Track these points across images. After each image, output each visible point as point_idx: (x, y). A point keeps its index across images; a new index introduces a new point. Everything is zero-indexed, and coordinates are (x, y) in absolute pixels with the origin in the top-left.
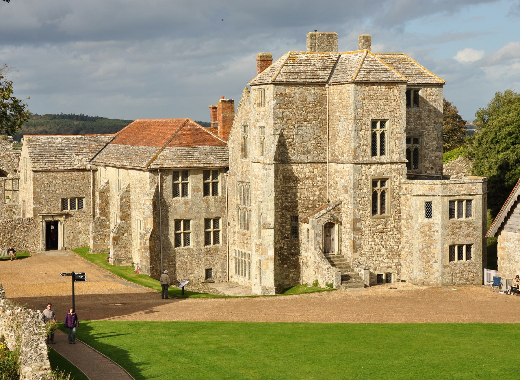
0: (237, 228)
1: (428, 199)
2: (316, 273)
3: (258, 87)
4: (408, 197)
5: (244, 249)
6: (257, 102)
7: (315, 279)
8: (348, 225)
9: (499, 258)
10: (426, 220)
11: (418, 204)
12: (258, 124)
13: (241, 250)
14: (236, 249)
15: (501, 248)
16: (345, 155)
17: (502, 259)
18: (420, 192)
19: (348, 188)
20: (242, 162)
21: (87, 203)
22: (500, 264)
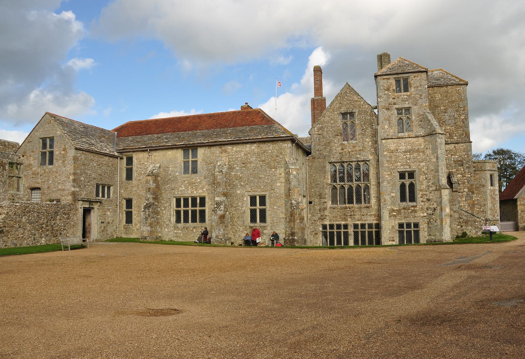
0: (329, 204)
1: (492, 172)
2: (462, 226)
3: (396, 76)
4: (477, 172)
5: (346, 220)
6: (391, 89)
7: (462, 232)
8: (466, 190)
9: (519, 212)
10: (492, 188)
11: (489, 177)
12: (397, 106)
13: (335, 223)
14: (327, 223)
15: (521, 205)
16: (455, 138)
17: (522, 211)
18: (489, 168)
19: (465, 162)
20: (342, 144)
21: (114, 192)
22: (520, 215)
